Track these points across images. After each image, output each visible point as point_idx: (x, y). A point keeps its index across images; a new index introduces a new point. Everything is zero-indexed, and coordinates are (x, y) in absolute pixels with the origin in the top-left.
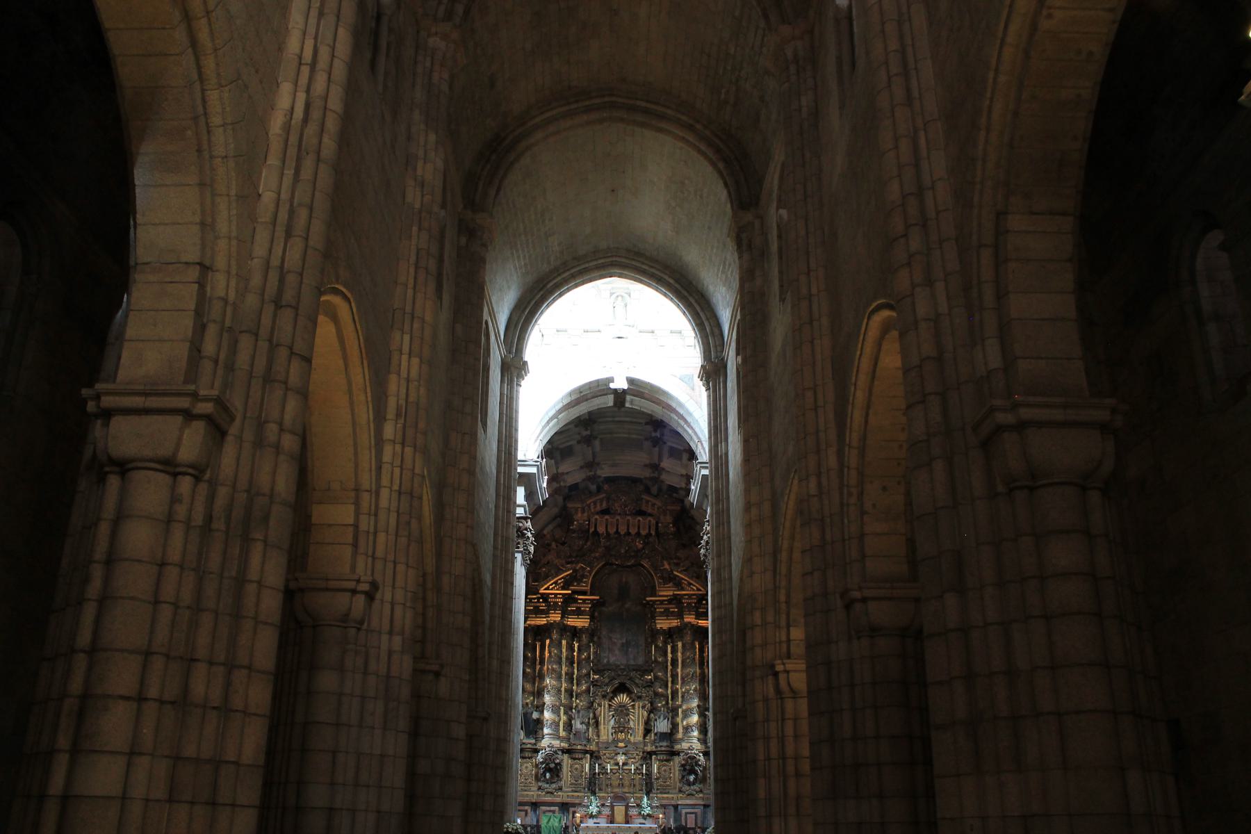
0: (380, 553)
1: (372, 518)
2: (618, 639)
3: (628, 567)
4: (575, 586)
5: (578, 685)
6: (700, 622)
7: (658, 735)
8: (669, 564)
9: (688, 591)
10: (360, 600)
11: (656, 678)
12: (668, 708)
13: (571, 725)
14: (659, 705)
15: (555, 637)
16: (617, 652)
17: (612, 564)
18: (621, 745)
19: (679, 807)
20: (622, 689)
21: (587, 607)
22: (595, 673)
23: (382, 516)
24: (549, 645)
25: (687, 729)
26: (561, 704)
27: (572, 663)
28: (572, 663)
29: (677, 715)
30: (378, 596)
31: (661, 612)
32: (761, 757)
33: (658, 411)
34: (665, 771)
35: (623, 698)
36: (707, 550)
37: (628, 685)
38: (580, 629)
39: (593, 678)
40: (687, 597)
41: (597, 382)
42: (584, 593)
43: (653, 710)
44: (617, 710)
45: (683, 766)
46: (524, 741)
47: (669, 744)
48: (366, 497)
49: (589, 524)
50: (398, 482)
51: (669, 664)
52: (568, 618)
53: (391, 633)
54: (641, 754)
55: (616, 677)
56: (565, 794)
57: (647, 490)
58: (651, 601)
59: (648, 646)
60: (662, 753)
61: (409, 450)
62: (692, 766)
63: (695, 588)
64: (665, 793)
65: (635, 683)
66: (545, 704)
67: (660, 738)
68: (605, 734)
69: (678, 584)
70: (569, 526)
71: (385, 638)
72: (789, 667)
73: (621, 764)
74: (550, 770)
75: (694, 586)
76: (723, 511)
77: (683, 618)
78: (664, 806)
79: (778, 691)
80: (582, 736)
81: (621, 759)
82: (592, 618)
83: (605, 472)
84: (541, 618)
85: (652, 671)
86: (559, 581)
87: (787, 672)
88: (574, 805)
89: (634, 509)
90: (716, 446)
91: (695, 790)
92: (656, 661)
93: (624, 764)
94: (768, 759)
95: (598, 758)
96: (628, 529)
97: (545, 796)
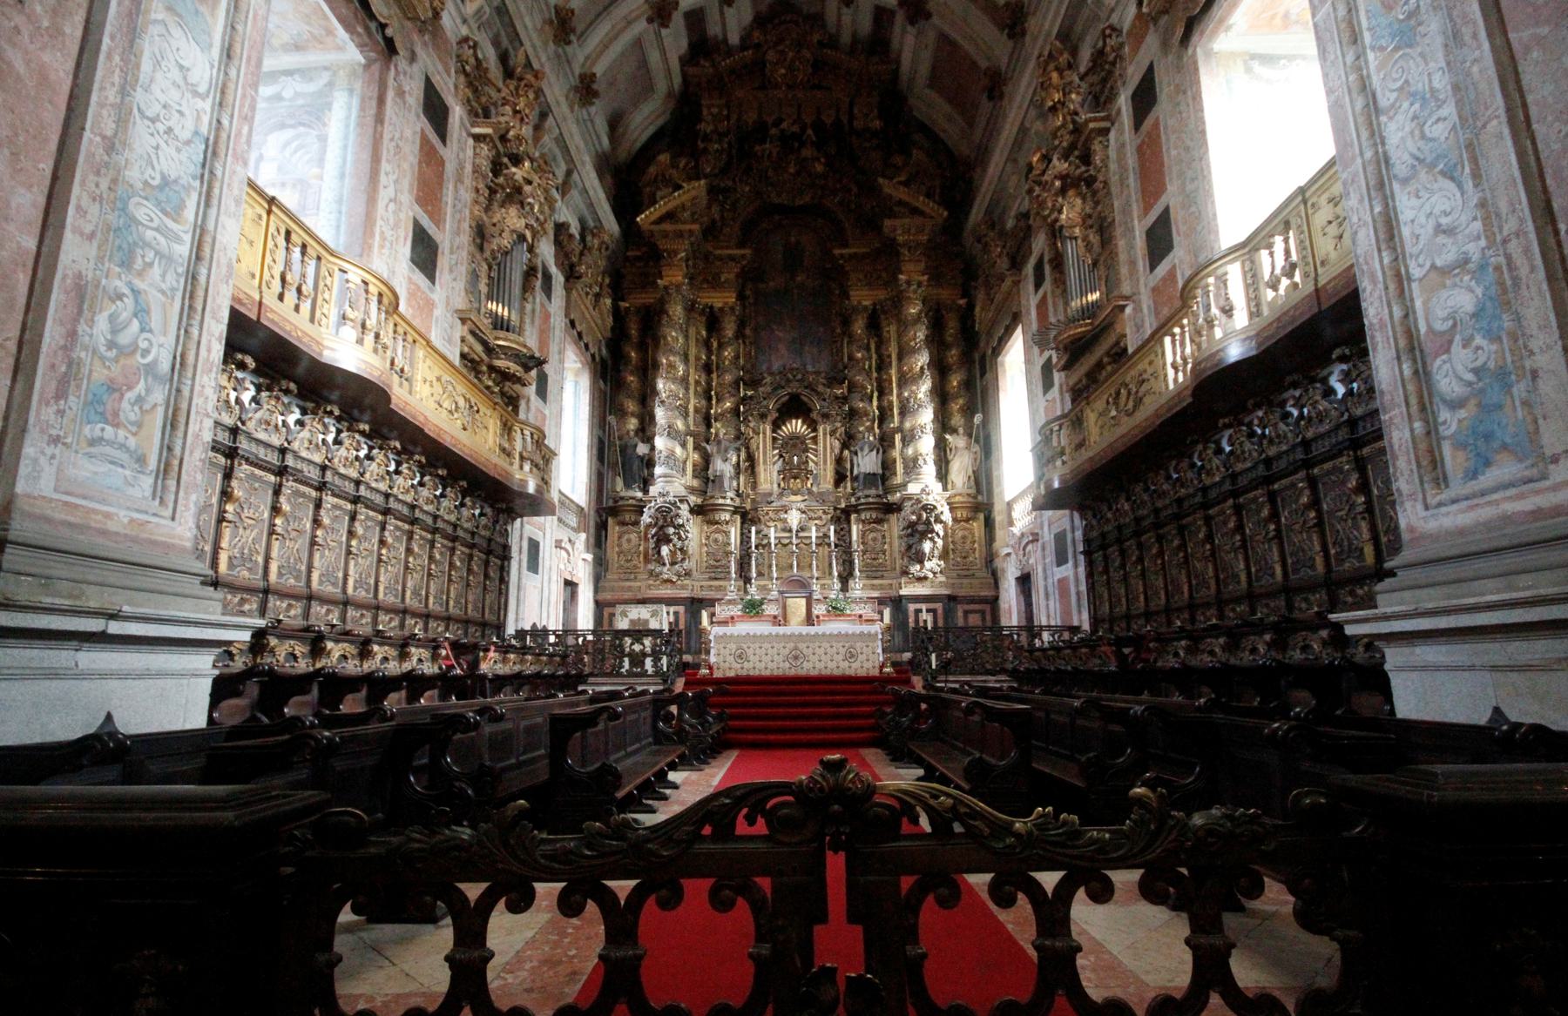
14: (861, 429)
16: (783, 351)
18: (793, 498)
20: (794, 407)
22: (748, 385)
25: (912, 465)
27: (707, 368)
29: (892, 445)
34: (874, 539)
35: (796, 426)
37: (805, 399)
38: (721, 309)
42: (727, 248)
43: (848, 441)
44: (787, 443)
45: (912, 525)
49: (728, 118)
55: (783, 383)
56: (697, 584)
58: (842, 256)
60: (870, 507)
62: (930, 523)
64: (876, 578)
65: (818, 393)
67: (864, 484)
68: (766, 480)
74: (668, 541)
80: (726, 484)
81: (794, 519)
82: (741, 297)
89: (809, 81)
92: (851, 358)
93: (802, 529)
95: (755, 521)
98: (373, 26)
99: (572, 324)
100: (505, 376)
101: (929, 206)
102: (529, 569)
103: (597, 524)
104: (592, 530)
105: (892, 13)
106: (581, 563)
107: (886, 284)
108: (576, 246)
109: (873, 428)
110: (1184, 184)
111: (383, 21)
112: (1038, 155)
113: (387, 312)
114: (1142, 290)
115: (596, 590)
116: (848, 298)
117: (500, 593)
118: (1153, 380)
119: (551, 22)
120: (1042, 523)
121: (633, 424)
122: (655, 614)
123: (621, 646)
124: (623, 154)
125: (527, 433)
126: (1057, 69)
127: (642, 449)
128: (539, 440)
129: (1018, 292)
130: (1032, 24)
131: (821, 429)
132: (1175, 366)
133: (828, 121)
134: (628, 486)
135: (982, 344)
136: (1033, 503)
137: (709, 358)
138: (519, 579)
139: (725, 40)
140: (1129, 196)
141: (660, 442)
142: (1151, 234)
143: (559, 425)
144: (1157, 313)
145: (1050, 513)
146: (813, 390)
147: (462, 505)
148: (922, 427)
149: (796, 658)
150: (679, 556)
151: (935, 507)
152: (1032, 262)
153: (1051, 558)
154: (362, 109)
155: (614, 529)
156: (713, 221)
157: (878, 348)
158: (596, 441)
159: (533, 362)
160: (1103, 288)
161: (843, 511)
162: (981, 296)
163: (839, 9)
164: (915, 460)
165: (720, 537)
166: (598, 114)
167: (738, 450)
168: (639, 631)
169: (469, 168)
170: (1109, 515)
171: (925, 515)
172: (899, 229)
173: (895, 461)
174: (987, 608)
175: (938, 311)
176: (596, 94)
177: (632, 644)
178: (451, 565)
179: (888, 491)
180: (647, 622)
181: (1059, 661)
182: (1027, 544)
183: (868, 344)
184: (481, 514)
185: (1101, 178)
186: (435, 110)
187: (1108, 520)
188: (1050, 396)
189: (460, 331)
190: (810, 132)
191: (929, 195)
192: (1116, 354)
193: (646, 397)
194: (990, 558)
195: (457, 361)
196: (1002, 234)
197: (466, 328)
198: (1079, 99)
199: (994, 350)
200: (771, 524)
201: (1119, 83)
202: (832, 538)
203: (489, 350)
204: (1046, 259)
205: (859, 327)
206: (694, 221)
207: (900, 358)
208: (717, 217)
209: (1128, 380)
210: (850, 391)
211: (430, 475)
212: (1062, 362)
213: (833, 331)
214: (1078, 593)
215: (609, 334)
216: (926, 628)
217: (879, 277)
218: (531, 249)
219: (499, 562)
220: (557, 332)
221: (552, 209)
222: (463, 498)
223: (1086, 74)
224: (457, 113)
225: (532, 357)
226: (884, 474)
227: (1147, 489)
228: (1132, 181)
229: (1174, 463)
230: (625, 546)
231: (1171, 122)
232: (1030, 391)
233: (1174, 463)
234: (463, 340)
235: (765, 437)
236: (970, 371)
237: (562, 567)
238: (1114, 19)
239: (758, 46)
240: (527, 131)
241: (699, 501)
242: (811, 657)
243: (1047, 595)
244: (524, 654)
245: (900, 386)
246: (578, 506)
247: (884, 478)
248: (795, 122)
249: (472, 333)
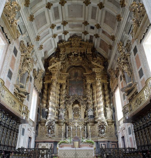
7: (89, 116)
11: (87, 98)
13: (59, 114)
16: (74, 92)
18: (76, 120)
19: (99, 142)
20: (76, 102)
25: (100, 113)
27: (60, 95)
34: (92, 129)
35: (77, 106)
37: (78, 101)
38: (63, 84)
43: (87, 109)
45: (100, 126)
46: (42, 119)
47: (93, 119)
49: (65, 52)
54: (84, 123)
58: (85, 74)
60: (91, 122)
62: (103, 125)
74: (50, 129)
75: (99, 67)
80: (63, 117)
81: (76, 125)
82: (67, 81)
91: (104, 135)
93: (77, 127)
98: (7, 40)
99: (35, 86)
100: (22, 96)
101: (100, 66)
102: (22, 135)
103: (36, 125)
104: (35, 126)
105: (93, 36)
106: (32, 133)
107: (93, 80)
108: (37, 73)
110: (144, 64)
111: (9, 39)
112: (119, 59)
113: (2, 86)
114: (139, 81)
115: (35, 140)
116: (86, 82)
117: (16, 140)
118: (143, 98)
119: (36, 38)
120: (125, 125)
121: (45, 105)
122: (47, 145)
123: (39, 152)
124: (46, 58)
125: (24, 107)
126: (121, 46)
127: (46, 110)
128: (27, 108)
129: (118, 81)
130: (116, 39)
131: (81, 106)
132: (146, 96)
133: (82, 52)
134: (43, 117)
135: (112, 90)
136: (123, 121)
137: (60, 93)
138: (20, 137)
139: (65, 40)
140: (135, 66)
141: (50, 109)
142: (139, 72)
143: (30, 105)
144: (142, 86)
145: (127, 123)
146: (80, 99)
147: (11, 121)
148: (101, 106)
150: (53, 132)
151: (104, 122)
152: (120, 76)
153: (128, 133)
154: (3, 52)
155: (40, 126)
156: (62, 68)
157: (92, 92)
158: (37, 108)
159: (27, 94)
160: (132, 81)
161: (86, 123)
162: (111, 82)
163: (84, 36)
166: (43, 51)
167: (65, 110)
168: (44, 149)
169: (20, 60)
170: (138, 124)
171: (102, 124)
172: (95, 70)
173: (96, 113)
174: (116, 144)
175: (103, 84)
176: (42, 48)
177: (42, 152)
178: (7, 134)
179: (95, 119)
180: (45, 146)
181: (131, 156)
182: (123, 130)
184: (14, 123)
185: (130, 63)
186: (15, 52)
187: (138, 125)
188: (125, 100)
189: (14, 88)
190: (79, 54)
192: (136, 93)
193: (48, 100)
194: (116, 133)
195: (13, 93)
196: (114, 71)
197: (15, 88)
198: (125, 50)
199: (114, 91)
200: (72, 126)
201: (131, 48)
203: (19, 91)
204: (122, 76)
205: (89, 87)
206: (58, 69)
207: (96, 93)
208: (63, 68)
209: (138, 98)
210: (87, 99)
211: (5, 115)
212: (127, 94)
213: (84, 88)
214: (134, 140)
215: (41, 88)
216: (103, 148)
217: (92, 78)
218: (29, 74)
219: (16, 133)
220: (32, 88)
221: (33, 66)
222: (11, 120)
223: (126, 46)
224: (19, 52)
225: (27, 93)
226: (94, 115)
227: (144, 119)
228: (135, 63)
229: (149, 114)
230: (42, 130)
231: (140, 55)
232: (121, 99)
233: (149, 114)
234: (15, 90)
235: (70, 108)
236: (110, 95)
237: (29, 134)
238: (129, 39)
240: (30, 54)
241: (57, 121)
242: (79, 155)
243: (128, 141)
244: (19, 154)
245: (96, 98)
246: (33, 121)
247: (94, 116)
248: (77, 52)
249: (16, 88)
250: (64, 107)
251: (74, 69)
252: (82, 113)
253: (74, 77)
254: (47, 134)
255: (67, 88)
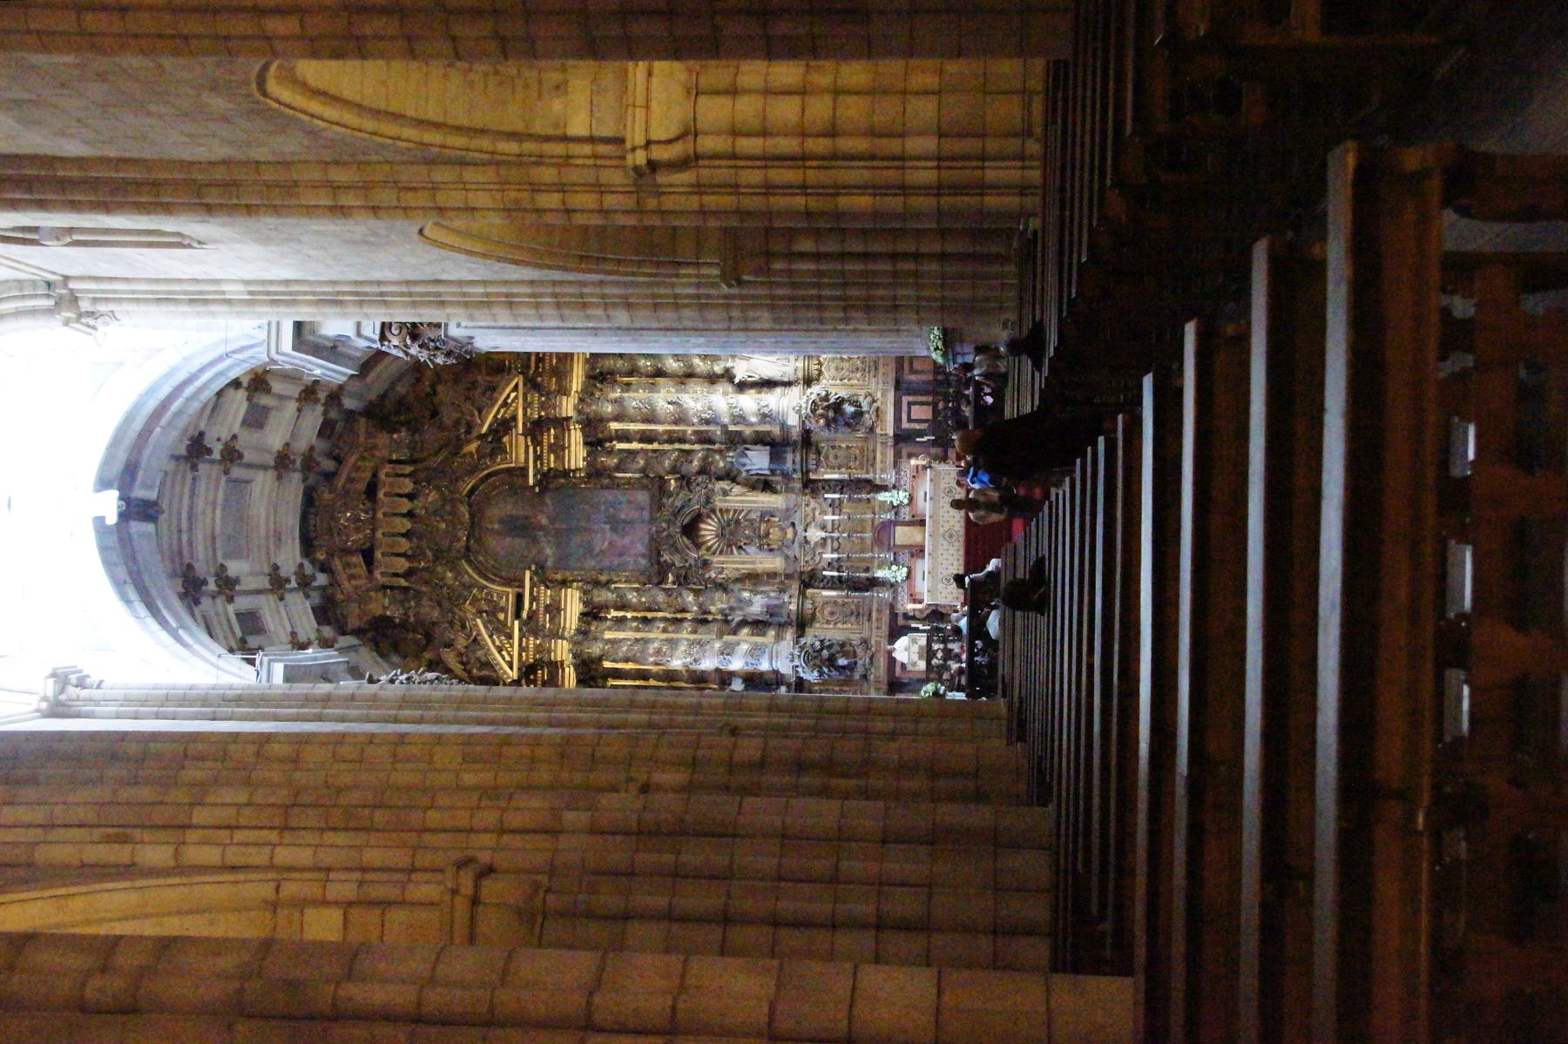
0: (400, 858)
1: (332, 875)
2: (603, 539)
3: (472, 516)
4: (506, 617)
5: (684, 610)
6: (574, 389)
7: (773, 467)
8: (469, 442)
9: (516, 409)
10: (492, 889)
12: (728, 449)
15: (595, 649)
16: (627, 540)
17: (468, 548)
18: (790, 532)
20: (691, 530)
21: (546, 595)
22: (663, 580)
23: (328, 858)
24: (614, 661)
25: (765, 417)
26: (720, 635)
28: (645, 620)
29: (739, 433)
30: (484, 857)
31: (556, 459)
32: (799, 202)
33: (169, 439)
34: (836, 457)
35: (709, 530)
36: (437, 348)
37: (686, 521)
38: (586, 604)
39: (674, 583)
40: (529, 411)
41: (103, 549)
42: (519, 598)
43: (730, 476)
44: (729, 540)
45: (828, 425)
48: (290, 889)
49: (392, 588)
50: (264, 833)
51: (650, 447)
52: (564, 628)
53: (554, 832)
54: (807, 498)
57: (329, 477)
58: (535, 475)
59: (616, 485)
61: (200, 816)
62: (828, 407)
63: (513, 395)
66: (717, 670)
69: (505, 425)
70: (395, 626)
71: (565, 842)
72: (640, 139)
73: (823, 534)
74: (831, 661)
75: (508, 396)
76: (357, 294)
77: (568, 419)
78: (898, 456)
79: (682, 164)
82: (565, 583)
83: (290, 558)
84: (563, 677)
85: (661, 478)
86: (498, 643)
87: (648, 143)
88: (894, 616)
90: (229, 302)
92: (643, 470)
93: (823, 528)
94: (804, 188)
96: (404, 515)
97: (877, 668)
109: (720, 452)
127: (737, 685)
141: (737, 664)
149: (951, 536)
150: (847, 648)
164: (764, 416)
165: (828, 609)
171: (820, 411)
173: (757, 432)
180: (921, 647)
183: (629, 452)
191: (493, 389)
200: (817, 558)
202: (837, 496)
235: (727, 562)
239: (330, 554)
250: (718, 595)
251: (479, 540)
252: (754, 502)
253: (535, 540)
254: (857, 676)
255: (603, 578)
